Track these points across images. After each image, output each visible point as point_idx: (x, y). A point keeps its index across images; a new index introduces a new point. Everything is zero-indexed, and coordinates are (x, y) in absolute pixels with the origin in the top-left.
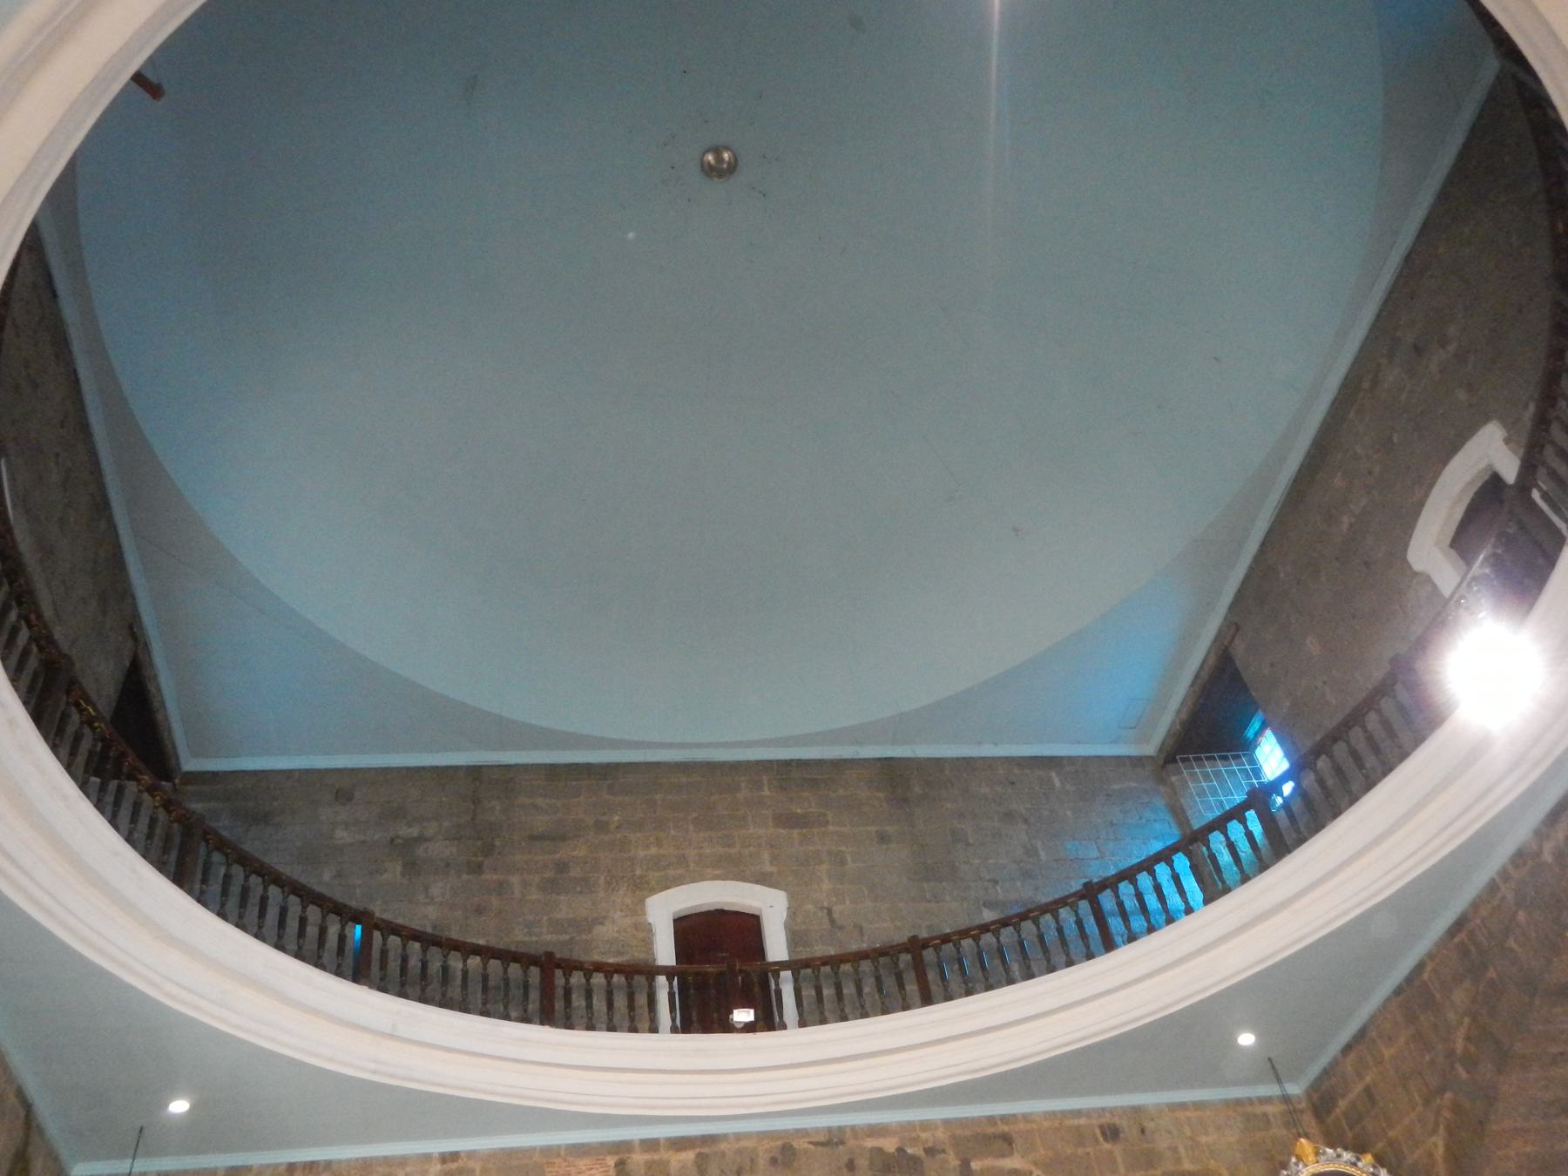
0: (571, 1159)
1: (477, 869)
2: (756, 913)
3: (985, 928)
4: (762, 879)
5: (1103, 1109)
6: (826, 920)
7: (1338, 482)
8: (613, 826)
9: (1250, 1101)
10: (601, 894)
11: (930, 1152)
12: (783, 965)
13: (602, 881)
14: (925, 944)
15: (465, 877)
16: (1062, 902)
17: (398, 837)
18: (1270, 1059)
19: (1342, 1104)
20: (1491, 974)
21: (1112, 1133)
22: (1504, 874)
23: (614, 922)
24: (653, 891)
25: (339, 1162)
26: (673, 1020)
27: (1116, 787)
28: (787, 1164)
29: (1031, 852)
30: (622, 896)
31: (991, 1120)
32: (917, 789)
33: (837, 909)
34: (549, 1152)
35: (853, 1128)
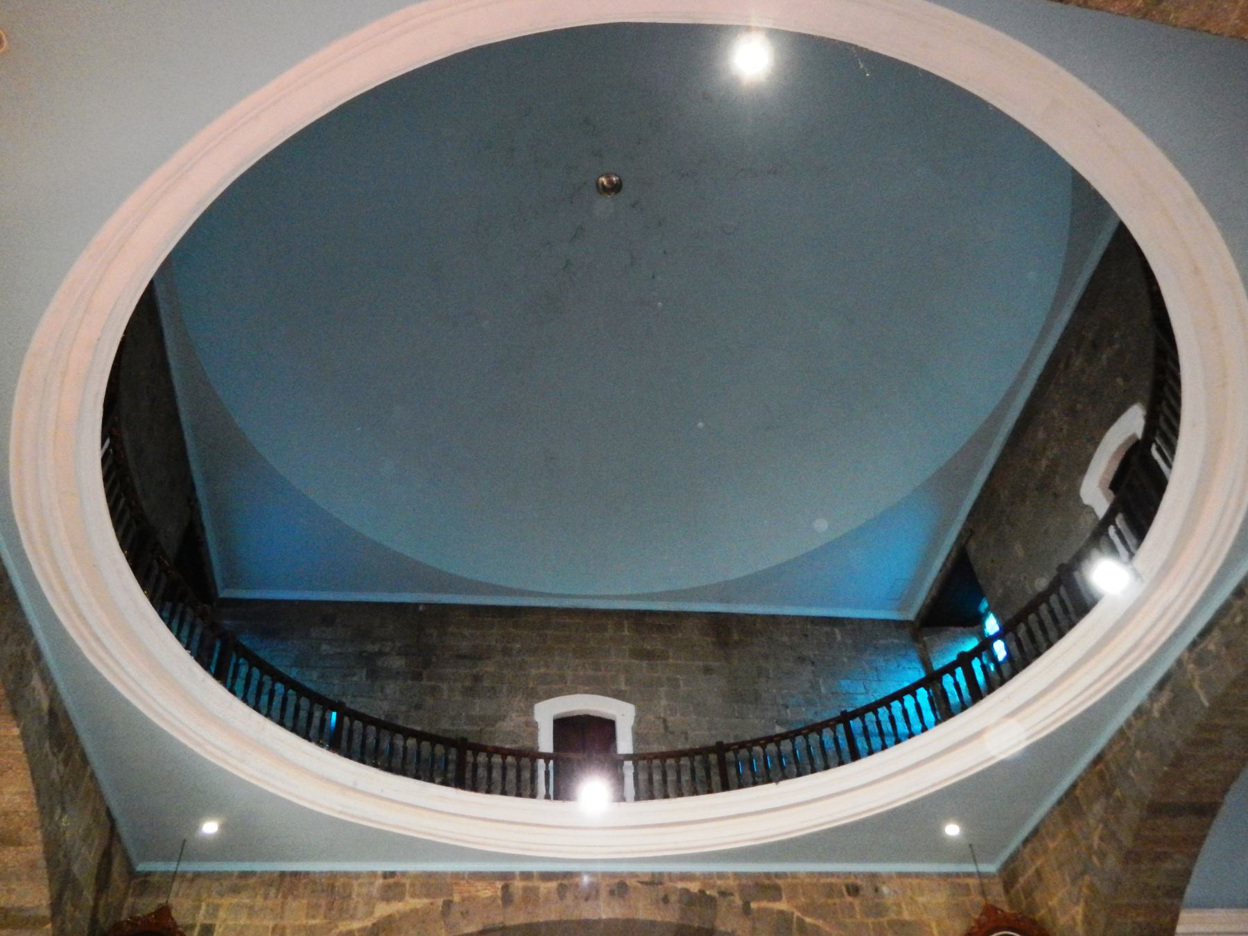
0: (472, 882)
1: (417, 677)
2: (613, 719)
3: (770, 739)
4: (618, 695)
5: (850, 873)
6: (662, 725)
7: (1041, 435)
8: (514, 652)
9: (958, 875)
10: (504, 700)
11: (723, 894)
12: (628, 757)
13: (505, 690)
14: (728, 747)
15: (410, 682)
16: (826, 724)
17: (364, 651)
18: (971, 846)
19: (1021, 880)
20: (1117, 793)
21: (854, 890)
22: (1129, 724)
23: (512, 720)
24: (540, 699)
25: (315, 873)
26: (547, 790)
27: (882, 642)
28: (622, 896)
29: (814, 686)
30: (519, 702)
31: (768, 875)
32: (736, 637)
33: (671, 719)
34: (457, 876)
35: (670, 874)
